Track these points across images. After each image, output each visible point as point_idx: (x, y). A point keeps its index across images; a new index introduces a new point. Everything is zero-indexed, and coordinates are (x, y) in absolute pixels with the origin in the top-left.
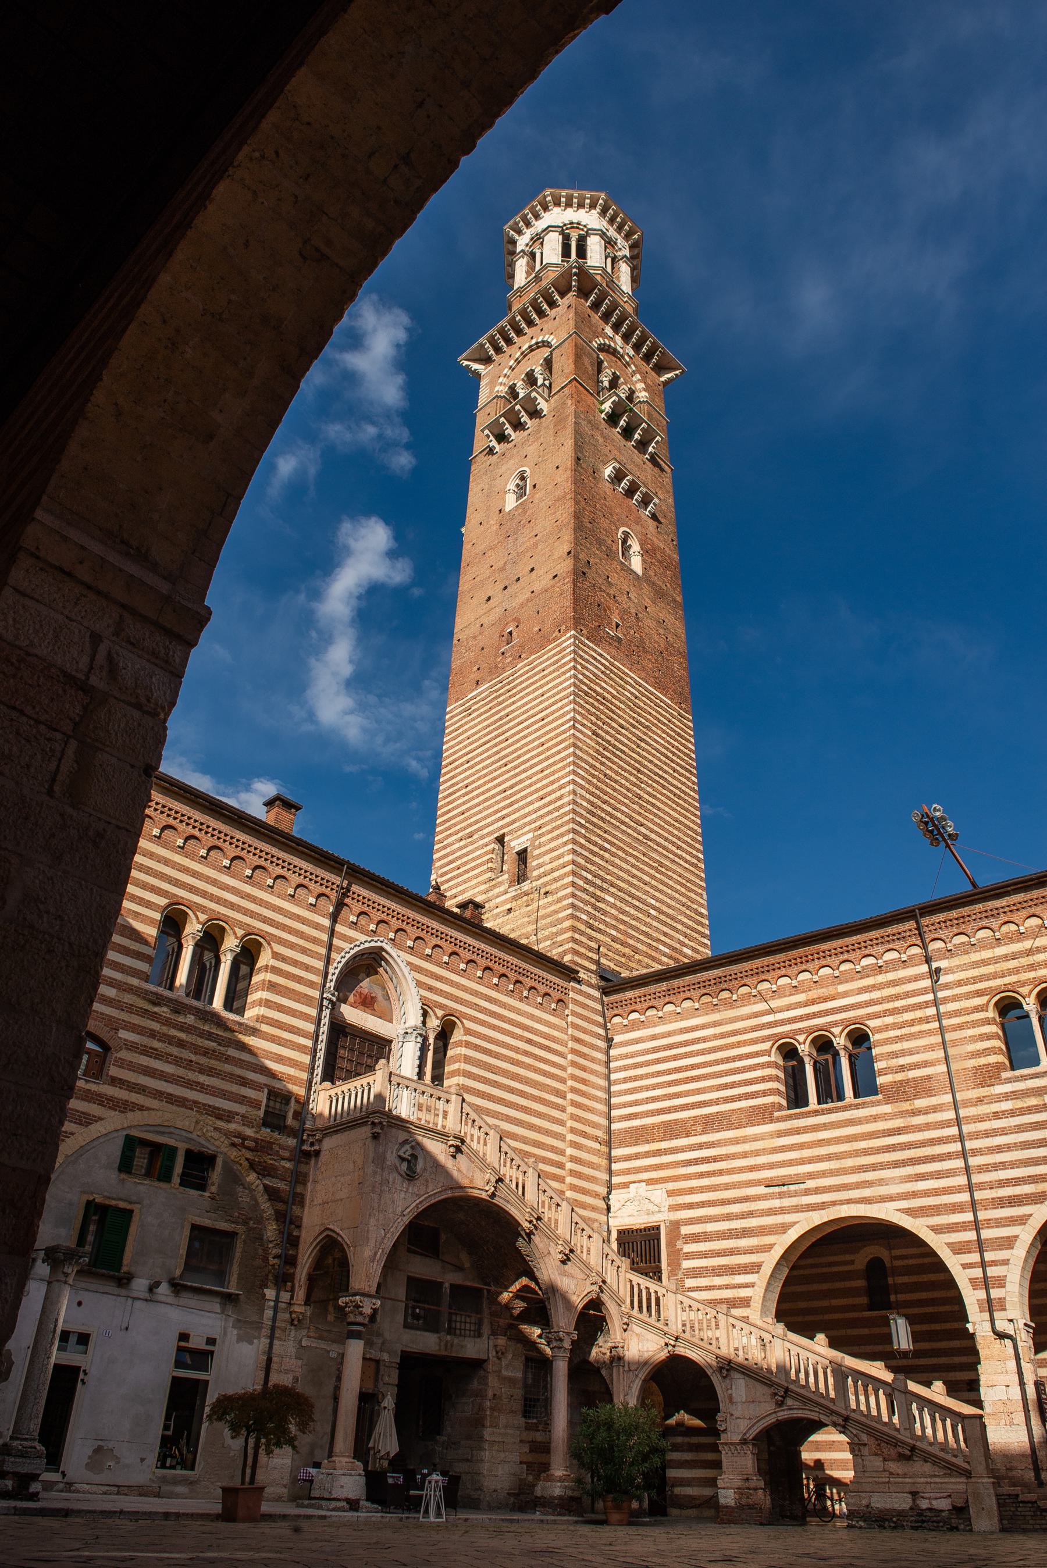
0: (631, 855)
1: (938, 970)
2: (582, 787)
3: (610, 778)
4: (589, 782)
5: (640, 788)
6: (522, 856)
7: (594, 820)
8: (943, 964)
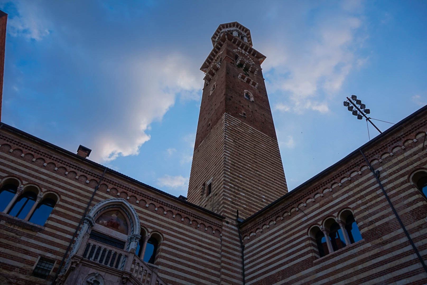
1: (379, 172)
2: (228, 156)
3: (242, 155)
4: (232, 155)
7: (235, 167)
8: (380, 169)
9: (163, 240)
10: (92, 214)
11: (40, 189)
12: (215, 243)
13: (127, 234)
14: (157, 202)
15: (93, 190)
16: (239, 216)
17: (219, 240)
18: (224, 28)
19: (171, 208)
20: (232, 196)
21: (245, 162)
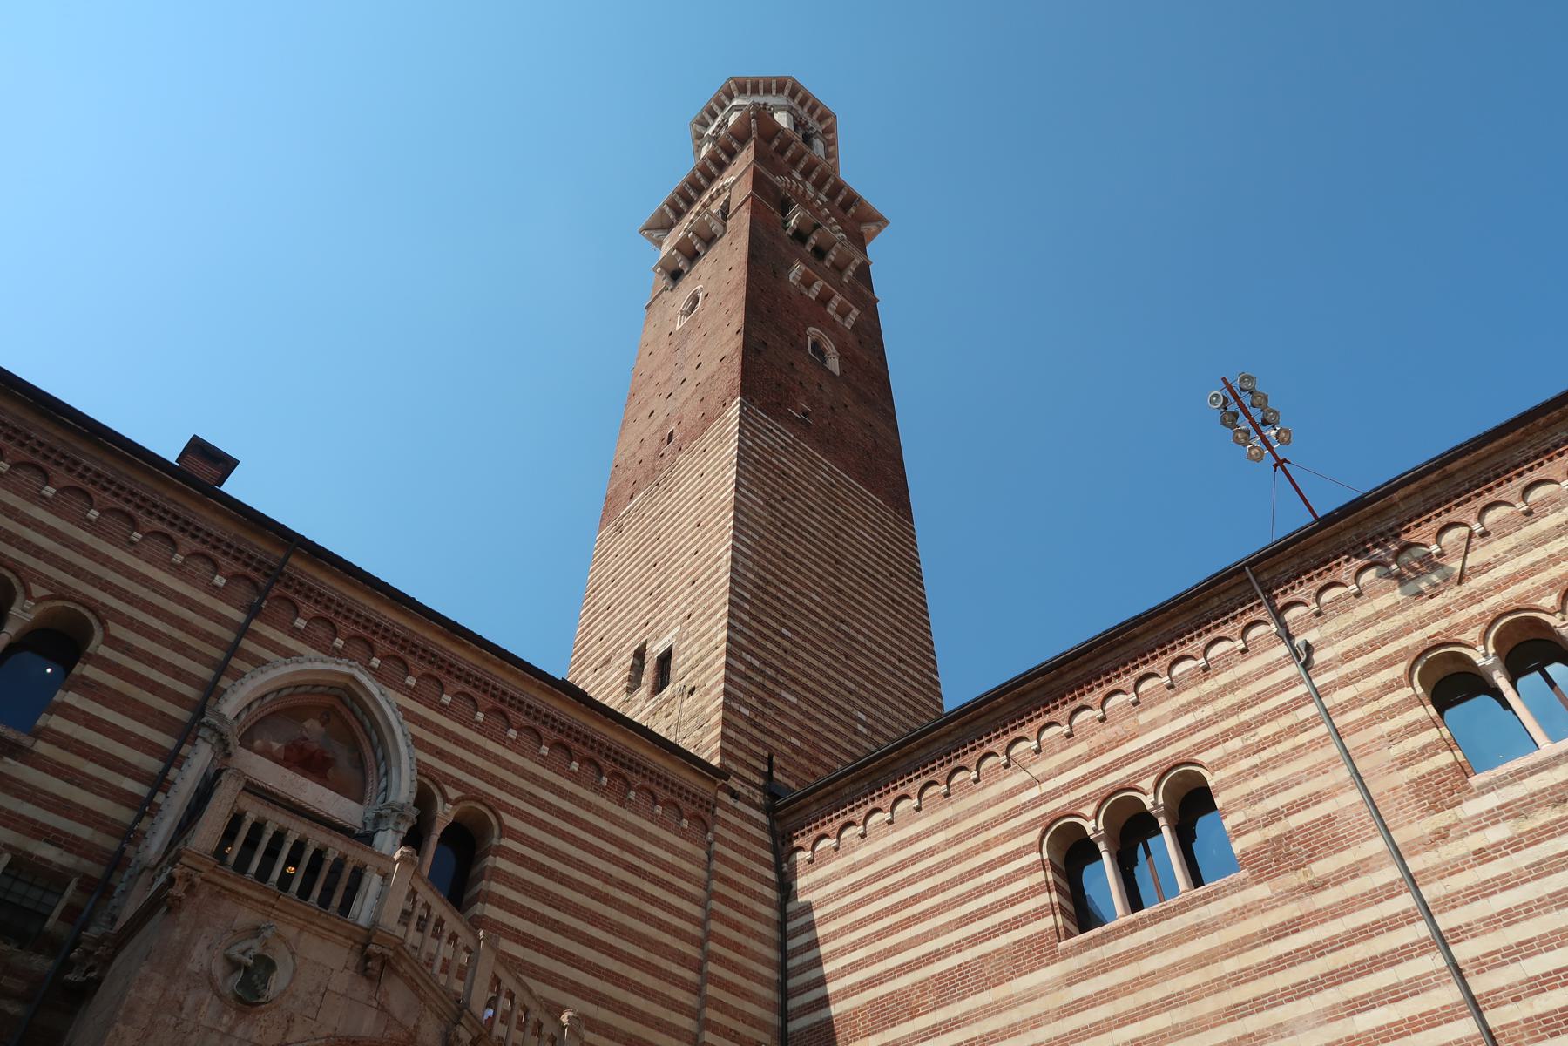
0: (824, 651)
2: (746, 556)
3: (793, 558)
4: (759, 554)
5: (839, 580)
6: (665, 660)
7: (767, 598)
8: (1312, 636)
9: (501, 836)
11: (24, 585)
12: (686, 866)
13: (361, 802)
14: (485, 692)
15: (239, 616)
16: (776, 775)
17: (702, 854)
18: (742, 91)
19: (536, 719)
20: (753, 701)
21: (801, 583)
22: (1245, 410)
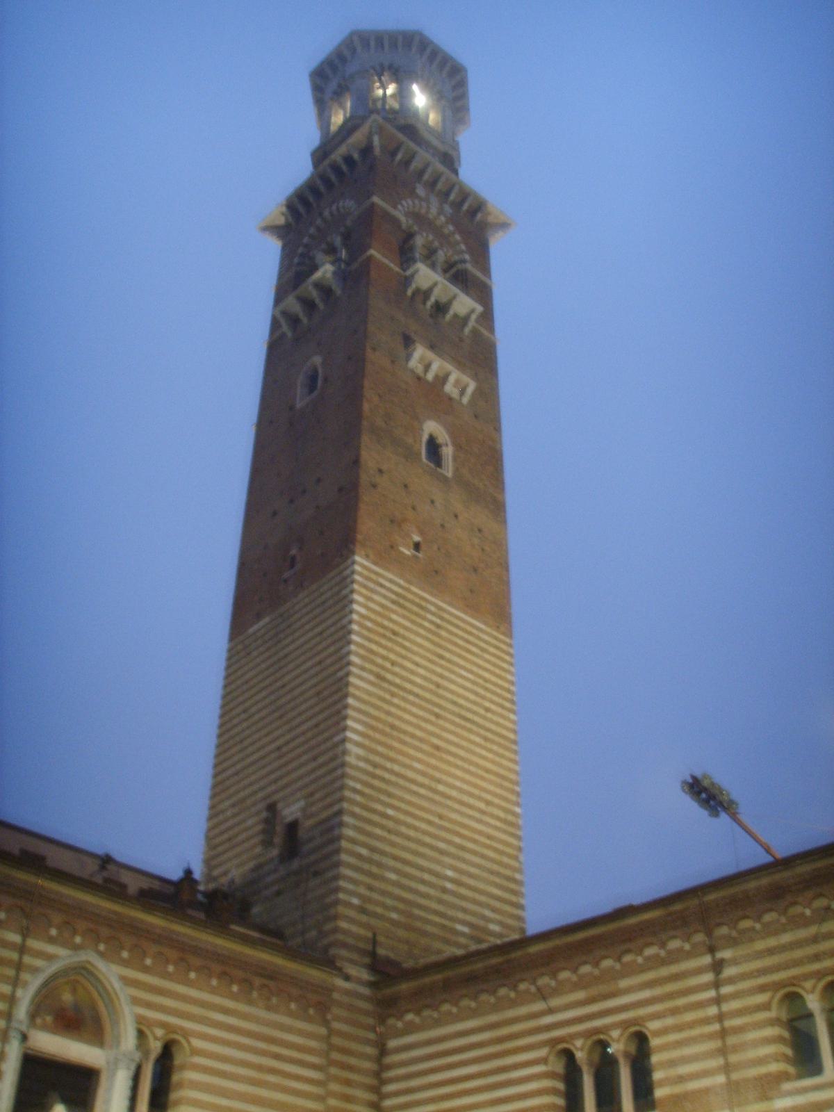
5: (439, 737)
10: (22, 1012)
17: (323, 1031)
22: (705, 793)
